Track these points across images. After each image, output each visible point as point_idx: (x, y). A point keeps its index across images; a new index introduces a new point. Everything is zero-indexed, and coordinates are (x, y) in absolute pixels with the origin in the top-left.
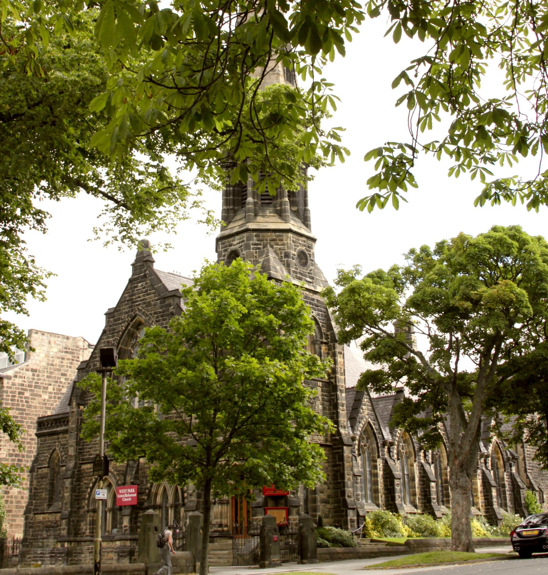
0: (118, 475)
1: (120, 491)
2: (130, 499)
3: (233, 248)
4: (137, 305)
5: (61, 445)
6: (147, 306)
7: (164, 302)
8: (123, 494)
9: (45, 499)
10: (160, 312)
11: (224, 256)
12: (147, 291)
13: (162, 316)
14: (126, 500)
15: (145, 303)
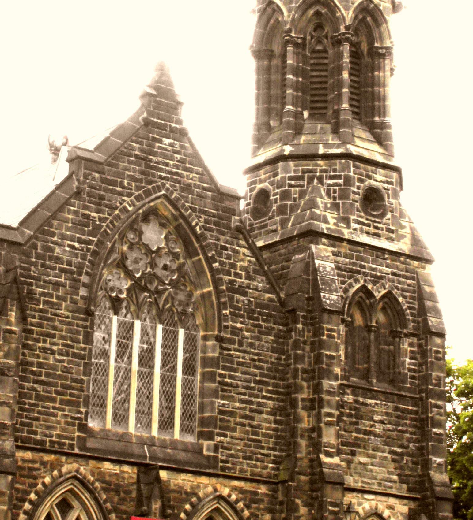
0: (104, 489)
3: (373, 182)
4: (160, 177)
6: (183, 190)
7: (221, 201)
10: (214, 216)
11: (359, 188)
12: (182, 161)
13: (216, 224)
15: (179, 183)
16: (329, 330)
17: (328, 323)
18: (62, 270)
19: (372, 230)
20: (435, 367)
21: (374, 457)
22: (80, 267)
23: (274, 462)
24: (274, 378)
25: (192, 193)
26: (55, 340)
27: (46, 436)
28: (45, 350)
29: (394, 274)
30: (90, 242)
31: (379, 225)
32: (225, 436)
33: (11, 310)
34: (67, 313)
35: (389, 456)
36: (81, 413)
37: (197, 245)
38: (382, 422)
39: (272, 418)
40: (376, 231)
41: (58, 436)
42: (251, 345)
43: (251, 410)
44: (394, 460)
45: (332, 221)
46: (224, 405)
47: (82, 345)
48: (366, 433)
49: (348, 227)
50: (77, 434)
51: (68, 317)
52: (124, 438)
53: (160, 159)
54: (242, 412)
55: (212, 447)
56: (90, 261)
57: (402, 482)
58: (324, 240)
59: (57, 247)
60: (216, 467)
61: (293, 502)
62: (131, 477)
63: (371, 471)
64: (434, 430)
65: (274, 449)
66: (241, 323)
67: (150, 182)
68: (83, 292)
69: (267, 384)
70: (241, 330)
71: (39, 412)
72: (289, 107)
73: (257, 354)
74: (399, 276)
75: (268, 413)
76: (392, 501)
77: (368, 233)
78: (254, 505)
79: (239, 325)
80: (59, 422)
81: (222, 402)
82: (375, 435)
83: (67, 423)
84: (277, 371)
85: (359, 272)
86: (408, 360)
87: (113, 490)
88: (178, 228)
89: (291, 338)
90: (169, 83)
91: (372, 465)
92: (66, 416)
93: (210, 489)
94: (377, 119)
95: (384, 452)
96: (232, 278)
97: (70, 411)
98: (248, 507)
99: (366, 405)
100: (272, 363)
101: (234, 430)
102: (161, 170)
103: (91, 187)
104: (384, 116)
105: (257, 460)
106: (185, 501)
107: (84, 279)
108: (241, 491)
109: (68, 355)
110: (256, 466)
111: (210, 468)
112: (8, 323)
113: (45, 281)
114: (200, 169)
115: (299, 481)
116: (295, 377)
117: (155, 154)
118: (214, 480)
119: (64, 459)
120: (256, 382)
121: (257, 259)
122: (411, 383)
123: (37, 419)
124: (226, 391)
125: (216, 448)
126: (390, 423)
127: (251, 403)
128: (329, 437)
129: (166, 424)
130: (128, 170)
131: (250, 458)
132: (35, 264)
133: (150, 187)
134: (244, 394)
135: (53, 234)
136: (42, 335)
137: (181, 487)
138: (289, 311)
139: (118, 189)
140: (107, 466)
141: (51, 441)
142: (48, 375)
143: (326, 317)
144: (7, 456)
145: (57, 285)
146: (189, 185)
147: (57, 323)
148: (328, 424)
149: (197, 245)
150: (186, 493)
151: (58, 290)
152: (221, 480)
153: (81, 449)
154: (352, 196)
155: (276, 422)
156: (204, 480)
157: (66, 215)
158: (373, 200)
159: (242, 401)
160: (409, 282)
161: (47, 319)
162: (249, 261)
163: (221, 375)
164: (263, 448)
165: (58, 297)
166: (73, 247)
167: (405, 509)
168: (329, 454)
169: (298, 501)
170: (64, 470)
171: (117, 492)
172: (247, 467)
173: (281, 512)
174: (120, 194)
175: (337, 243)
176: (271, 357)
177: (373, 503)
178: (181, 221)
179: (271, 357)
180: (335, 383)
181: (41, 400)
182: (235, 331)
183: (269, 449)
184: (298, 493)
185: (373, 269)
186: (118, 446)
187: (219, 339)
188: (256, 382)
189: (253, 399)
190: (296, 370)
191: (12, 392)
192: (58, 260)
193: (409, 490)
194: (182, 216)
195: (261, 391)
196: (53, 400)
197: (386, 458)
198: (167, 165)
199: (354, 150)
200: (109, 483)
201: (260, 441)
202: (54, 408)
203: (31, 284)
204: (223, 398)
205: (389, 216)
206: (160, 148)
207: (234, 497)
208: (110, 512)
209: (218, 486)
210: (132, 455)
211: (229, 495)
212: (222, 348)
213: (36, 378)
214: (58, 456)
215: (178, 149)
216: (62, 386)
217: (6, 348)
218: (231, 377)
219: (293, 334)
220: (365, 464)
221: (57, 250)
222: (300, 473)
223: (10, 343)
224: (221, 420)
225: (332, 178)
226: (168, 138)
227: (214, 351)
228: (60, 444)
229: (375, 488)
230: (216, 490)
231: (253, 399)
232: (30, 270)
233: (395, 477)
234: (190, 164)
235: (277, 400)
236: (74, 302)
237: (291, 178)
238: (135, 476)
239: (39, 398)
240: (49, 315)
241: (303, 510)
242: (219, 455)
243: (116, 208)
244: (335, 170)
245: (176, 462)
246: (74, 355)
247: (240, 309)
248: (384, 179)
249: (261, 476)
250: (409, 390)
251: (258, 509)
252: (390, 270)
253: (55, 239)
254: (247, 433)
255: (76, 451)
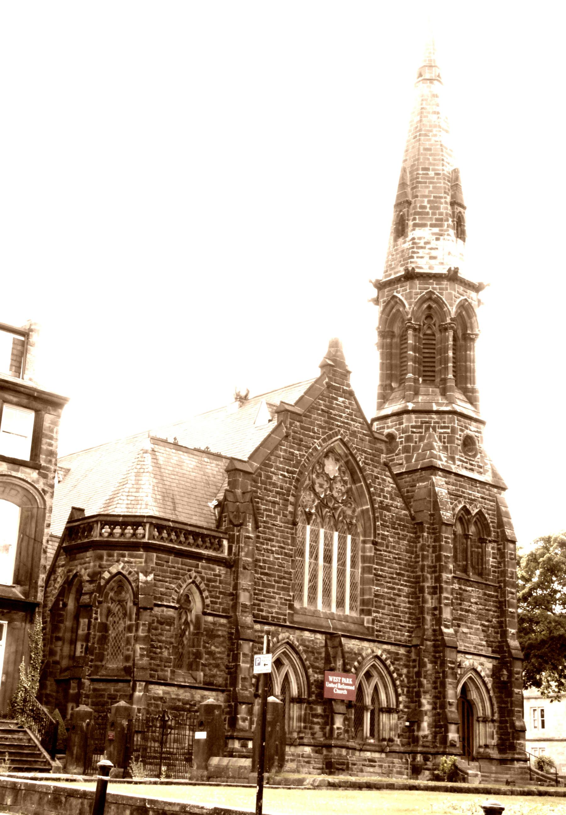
0: (306, 652)
1: (331, 678)
2: (345, 692)
3: (467, 432)
4: (337, 426)
5: (202, 578)
8: (335, 683)
9: (168, 660)
12: (350, 414)
13: (372, 460)
14: (339, 692)
16: (446, 538)
17: (445, 533)
18: (278, 493)
19: (468, 466)
20: (510, 565)
21: (471, 628)
22: (289, 490)
23: (408, 631)
24: (408, 571)
25: (356, 437)
26: (274, 543)
27: (269, 613)
28: (267, 550)
29: (482, 498)
30: (293, 472)
31: (473, 463)
32: (378, 612)
33: (249, 522)
34: (281, 524)
35: (480, 627)
36: (290, 596)
37: (360, 475)
38: (476, 603)
39: (407, 600)
40: (471, 467)
41: (277, 613)
42: (394, 547)
43: (394, 594)
44: (483, 631)
45: (444, 459)
46: (377, 591)
47: (291, 547)
48: (467, 611)
49: (454, 464)
50: (288, 611)
51: (281, 527)
52: (315, 613)
53: (337, 413)
54: (388, 595)
55: (371, 621)
56: (294, 486)
57: (488, 646)
58: (440, 473)
59: (274, 476)
60: (373, 635)
61: (423, 660)
62: (321, 643)
63: (470, 638)
64: (510, 610)
65: (408, 622)
66: (388, 531)
67: (331, 429)
68: (290, 508)
69: (403, 575)
70: (387, 536)
71: (264, 596)
72: (410, 375)
73: (397, 554)
74: (485, 499)
75: (405, 596)
76: (483, 659)
77: (466, 468)
78: (396, 662)
79: (386, 533)
80: (277, 603)
81: (377, 588)
82: (473, 613)
83: (282, 603)
84: (410, 566)
85: (461, 496)
86: (491, 559)
87: (311, 652)
88: (347, 463)
89: (419, 542)
90: (342, 357)
91: (470, 634)
92: (281, 598)
93: (369, 651)
94: (469, 386)
95: (477, 625)
96: (381, 499)
97: (284, 595)
98: (393, 663)
99: (466, 591)
100: (406, 560)
101: (383, 608)
102: (337, 420)
103: (295, 432)
104: (474, 384)
105: (398, 630)
106: (354, 659)
107: (291, 499)
108: (389, 652)
109: (282, 555)
110: (397, 634)
111: (367, 635)
112: (247, 531)
113: (267, 501)
114: (361, 420)
115: (427, 645)
116: (422, 570)
117: (333, 409)
118: (372, 644)
119: (280, 629)
120: (398, 574)
121: (397, 485)
122: (493, 576)
123: (263, 601)
124: (378, 580)
125: (373, 621)
126: (481, 604)
127: (394, 589)
128: (447, 614)
129: (340, 603)
130: (317, 420)
131: (393, 629)
132: (260, 488)
133: (331, 432)
134: (390, 582)
135: (271, 466)
136: (266, 540)
137: (352, 650)
138: (417, 524)
139: (311, 434)
140: (307, 634)
141: (272, 617)
142: (269, 568)
143: (444, 528)
144: (249, 628)
145: (274, 503)
146: (355, 432)
147: (275, 531)
148: (446, 605)
149: (360, 475)
150: (355, 654)
151: (275, 507)
152: (376, 644)
153: (291, 623)
154: (456, 441)
155: (409, 602)
156: (366, 644)
157: (279, 452)
158: (469, 444)
159: (389, 588)
160: (492, 503)
161: (269, 528)
162: (392, 487)
163: (375, 569)
164: (401, 621)
165: (275, 512)
166: (284, 476)
167: (490, 666)
168: (447, 627)
169: (426, 660)
170: (280, 637)
171: (313, 653)
172: (392, 635)
173: (414, 667)
174: (313, 437)
175: (448, 475)
176: (406, 556)
177: (471, 661)
178: (350, 457)
179: (406, 556)
180: (450, 576)
181: (266, 587)
182: (384, 537)
183: (405, 622)
184: (426, 654)
185: (470, 494)
186: (313, 620)
187: (375, 543)
188: (398, 574)
189: (396, 587)
190: (423, 566)
191: (250, 581)
192: (275, 485)
193: (493, 652)
194: (351, 454)
195: (400, 580)
196: (273, 587)
197: (478, 629)
198: (341, 416)
199: (459, 409)
200: (307, 647)
201: (400, 617)
202: (274, 593)
203: (258, 503)
204: (377, 585)
205: (479, 456)
206: (337, 404)
207: (384, 657)
208: (309, 668)
209: (375, 649)
210: (321, 627)
211: (382, 655)
212: (376, 550)
213: (262, 570)
214: (277, 628)
215: (348, 405)
216: (279, 576)
217: (246, 550)
218: (382, 570)
219: (421, 539)
220: (466, 633)
221: (274, 478)
222: (426, 640)
223: (249, 546)
224: (376, 601)
225: (442, 428)
226: (341, 397)
227: (371, 551)
228: (278, 619)
229: (472, 650)
230: (373, 652)
231: (396, 587)
232: (257, 492)
233: (484, 643)
234: (355, 416)
235: (410, 587)
236: (285, 516)
237: (413, 427)
238: (324, 642)
239: (264, 585)
240: (270, 525)
241: (429, 666)
242: (375, 626)
243: (310, 448)
244: (444, 422)
245: (349, 631)
246: (286, 554)
247: (386, 522)
248: (476, 429)
249: (400, 641)
250: (492, 581)
251: (399, 665)
252: (479, 495)
253: (273, 470)
254: (391, 610)
255: (288, 624)
